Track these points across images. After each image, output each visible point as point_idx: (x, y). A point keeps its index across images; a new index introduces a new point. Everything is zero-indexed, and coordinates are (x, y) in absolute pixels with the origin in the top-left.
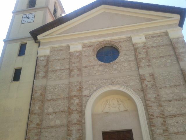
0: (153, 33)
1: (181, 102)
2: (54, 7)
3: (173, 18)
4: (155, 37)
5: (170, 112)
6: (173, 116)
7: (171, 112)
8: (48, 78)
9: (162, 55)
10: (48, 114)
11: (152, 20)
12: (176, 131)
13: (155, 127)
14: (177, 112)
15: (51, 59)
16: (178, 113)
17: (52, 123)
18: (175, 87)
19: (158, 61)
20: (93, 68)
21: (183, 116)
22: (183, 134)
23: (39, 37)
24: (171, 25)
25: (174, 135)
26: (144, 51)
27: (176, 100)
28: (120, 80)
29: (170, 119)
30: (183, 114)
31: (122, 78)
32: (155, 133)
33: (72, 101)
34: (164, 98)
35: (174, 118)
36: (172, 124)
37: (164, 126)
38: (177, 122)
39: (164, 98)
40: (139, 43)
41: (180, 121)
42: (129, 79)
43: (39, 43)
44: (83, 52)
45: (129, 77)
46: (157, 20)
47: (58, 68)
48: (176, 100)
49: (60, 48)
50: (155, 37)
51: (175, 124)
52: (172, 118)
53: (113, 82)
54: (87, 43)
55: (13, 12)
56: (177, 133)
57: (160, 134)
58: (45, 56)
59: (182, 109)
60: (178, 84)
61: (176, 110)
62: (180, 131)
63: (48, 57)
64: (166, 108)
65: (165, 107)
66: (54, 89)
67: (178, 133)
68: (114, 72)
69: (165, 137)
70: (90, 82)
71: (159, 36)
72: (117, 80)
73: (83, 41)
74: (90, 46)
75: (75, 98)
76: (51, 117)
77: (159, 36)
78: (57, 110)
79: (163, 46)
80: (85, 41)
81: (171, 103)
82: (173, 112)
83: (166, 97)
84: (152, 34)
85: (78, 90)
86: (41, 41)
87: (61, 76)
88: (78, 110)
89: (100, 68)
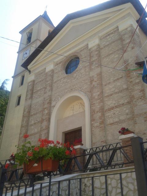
0: (106, 32)
1: (120, 94)
3: (125, 8)
4: (109, 35)
5: (109, 105)
6: (111, 109)
7: (110, 106)
8: (33, 98)
9: (112, 52)
10: (32, 125)
11: (108, 18)
12: (112, 122)
13: (94, 121)
14: (115, 104)
15: (36, 82)
16: (116, 105)
17: (33, 132)
18: (118, 80)
19: (108, 59)
20: (60, 81)
21: (119, 107)
22: (117, 124)
23: (29, 67)
24: (124, 16)
25: (109, 125)
26: (96, 53)
27: (116, 93)
28: (76, 86)
29: (109, 112)
30: (120, 105)
31: (78, 84)
32: (94, 126)
33: (44, 113)
34: (107, 93)
35: (112, 110)
36: (110, 117)
37: (101, 119)
38: (114, 114)
39: (107, 93)
40: (94, 47)
41: (117, 112)
42: (83, 83)
43: (30, 72)
44: (55, 70)
45: (83, 82)
46: (110, 17)
47: (39, 88)
48: (116, 93)
49: (42, 72)
50: (109, 35)
51: (112, 116)
52: (110, 111)
53: (72, 90)
54: (58, 61)
55: (18, 53)
56: (113, 123)
57: (97, 127)
58: (31, 81)
59: (119, 101)
60: (120, 76)
61: (115, 102)
62: (115, 122)
63: (34, 81)
64: (107, 103)
65: (106, 102)
66: (35, 106)
67: (113, 123)
68: (74, 80)
69: (100, 128)
70: (57, 94)
71: (112, 33)
72: (75, 87)
73: (35, 72)
74: (60, 63)
75: (45, 110)
76: (32, 127)
77: (112, 33)
78: (36, 122)
79: (114, 42)
80: (101, 34)
81: (112, 96)
82: (112, 105)
83: (109, 92)
84: (106, 33)
85: (48, 103)
86: (31, 70)
87: (40, 94)
89: (65, 81)
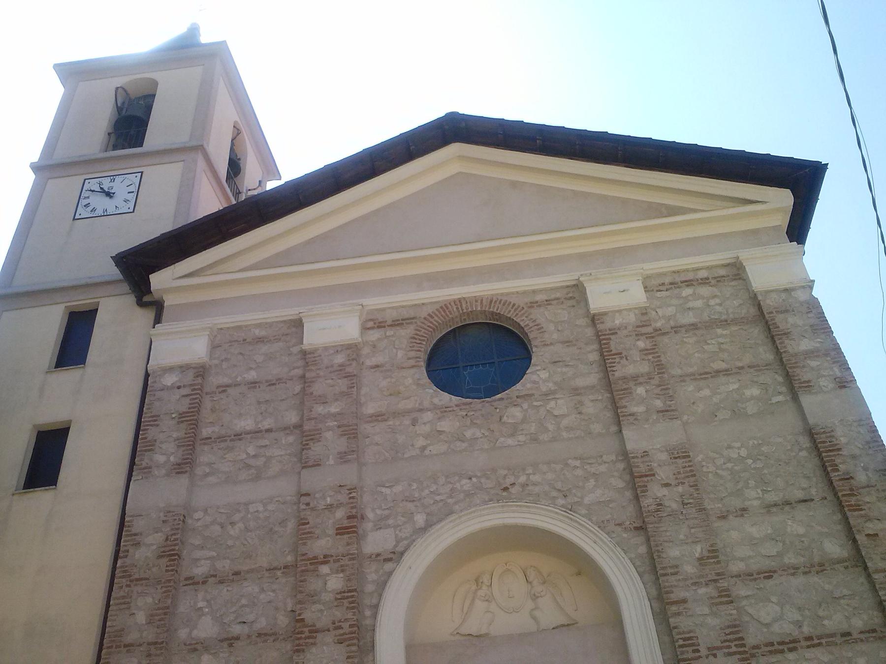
1: (814, 579)
2: (232, 149)
3: (766, 202)
4: (689, 283)
5: (768, 625)
6: (785, 647)
7: (776, 628)
8: (199, 471)
9: (723, 366)
14: (799, 624)
15: (215, 380)
16: (806, 630)
18: (787, 508)
19: (706, 392)
20: (414, 422)
21: (828, 644)
23: (159, 280)
24: (755, 232)
26: (641, 344)
27: (794, 570)
28: (536, 478)
31: (544, 468)
33: (314, 584)
34: (742, 560)
39: (742, 560)
40: (620, 311)
42: (579, 472)
43: (158, 309)
44: (366, 351)
45: (578, 463)
46: (695, 211)
47: (246, 424)
48: (794, 570)
49: (257, 332)
50: (689, 283)
53: (506, 489)
54: (383, 310)
55: (36, 168)
58: (183, 368)
59: (821, 613)
60: (800, 495)
61: (797, 617)
63: (201, 371)
64: (750, 610)
65: (744, 603)
66: (222, 526)
68: (510, 441)
70: (398, 489)
71: (705, 281)
72: (523, 479)
74: (398, 323)
75: (325, 569)
77: (705, 281)
78: (237, 629)
79: (725, 323)
80: (374, 302)
81: (771, 582)
82: (784, 629)
83: (750, 557)
85: (341, 531)
86: (169, 301)
87: (260, 462)
88: (340, 628)
89: (445, 425)
